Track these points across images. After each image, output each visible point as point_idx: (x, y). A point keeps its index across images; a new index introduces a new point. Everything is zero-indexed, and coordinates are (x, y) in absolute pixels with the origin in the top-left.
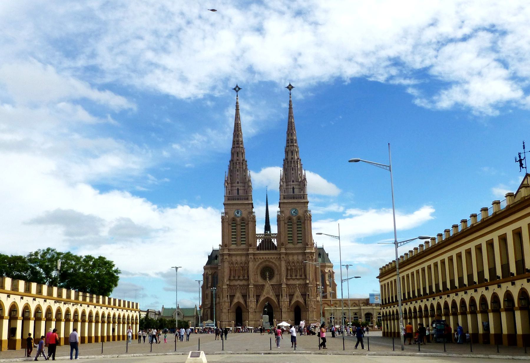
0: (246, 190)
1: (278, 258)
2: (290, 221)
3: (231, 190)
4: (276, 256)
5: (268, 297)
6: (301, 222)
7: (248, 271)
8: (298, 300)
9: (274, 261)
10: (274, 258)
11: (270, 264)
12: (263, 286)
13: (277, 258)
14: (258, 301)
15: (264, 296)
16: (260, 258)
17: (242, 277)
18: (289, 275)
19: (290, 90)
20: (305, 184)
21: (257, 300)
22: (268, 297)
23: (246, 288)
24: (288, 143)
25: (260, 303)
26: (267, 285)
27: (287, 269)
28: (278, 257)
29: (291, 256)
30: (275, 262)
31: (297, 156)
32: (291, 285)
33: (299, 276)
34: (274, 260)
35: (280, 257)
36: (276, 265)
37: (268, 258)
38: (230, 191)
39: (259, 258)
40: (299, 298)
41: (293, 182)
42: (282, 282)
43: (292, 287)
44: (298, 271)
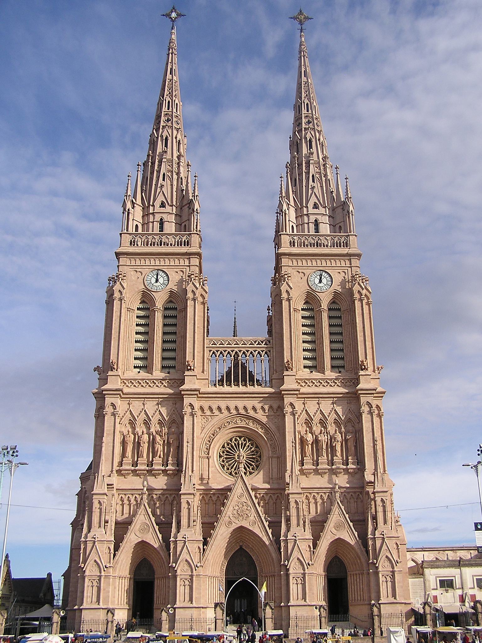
0: (183, 224)
1: (275, 406)
5: (241, 527)
6: (339, 310)
11: (251, 425)
12: (225, 493)
16: (219, 409)
18: (308, 460)
20: (348, 212)
21: (205, 539)
22: (241, 529)
23: (170, 499)
24: (300, 124)
26: (238, 490)
27: (303, 442)
29: (315, 402)
31: (323, 152)
32: (316, 491)
33: (339, 463)
35: (279, 407)
39: (214, 407)
41: (316, 206)
42: (287, 480)
44: (338, 448)
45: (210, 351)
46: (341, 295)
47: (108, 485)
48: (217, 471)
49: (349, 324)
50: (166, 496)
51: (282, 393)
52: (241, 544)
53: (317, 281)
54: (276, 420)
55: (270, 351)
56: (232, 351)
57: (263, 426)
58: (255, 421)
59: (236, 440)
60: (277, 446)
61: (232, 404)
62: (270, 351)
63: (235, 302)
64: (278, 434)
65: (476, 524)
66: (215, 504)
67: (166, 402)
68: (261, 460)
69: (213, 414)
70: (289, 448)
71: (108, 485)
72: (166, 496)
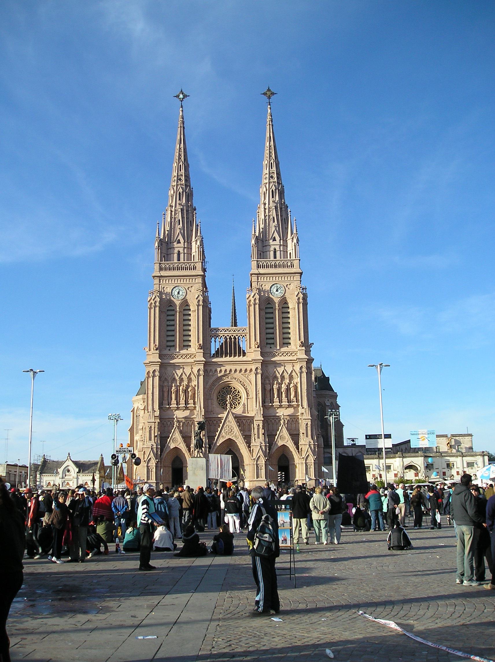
2: (269, 306)
3: (167, 255)
4: (244, 367)
7: (194, 393)
8: (285, 444)
14: (212, 446)
15: (223, 436)
17: (183, 404)
19: (269, 98)
22: (230, 439)
25: (215, 450)
32: (272, 417)
38: (165, 255)
39: (214, 370)
40: (286, 440)
43: (273, 421)
45: (211, 336)
47: (155, 416)
50: (188, 422)
52: (230, 448)
53: (275, 290)
55: (246, 335)
56: (224, 336)
59: (226, 389)
62: (246, 335)
63: (233, 275)
65: (366, 436)
66: (216, 425)
71: (155, 416)
72: (188, 422)
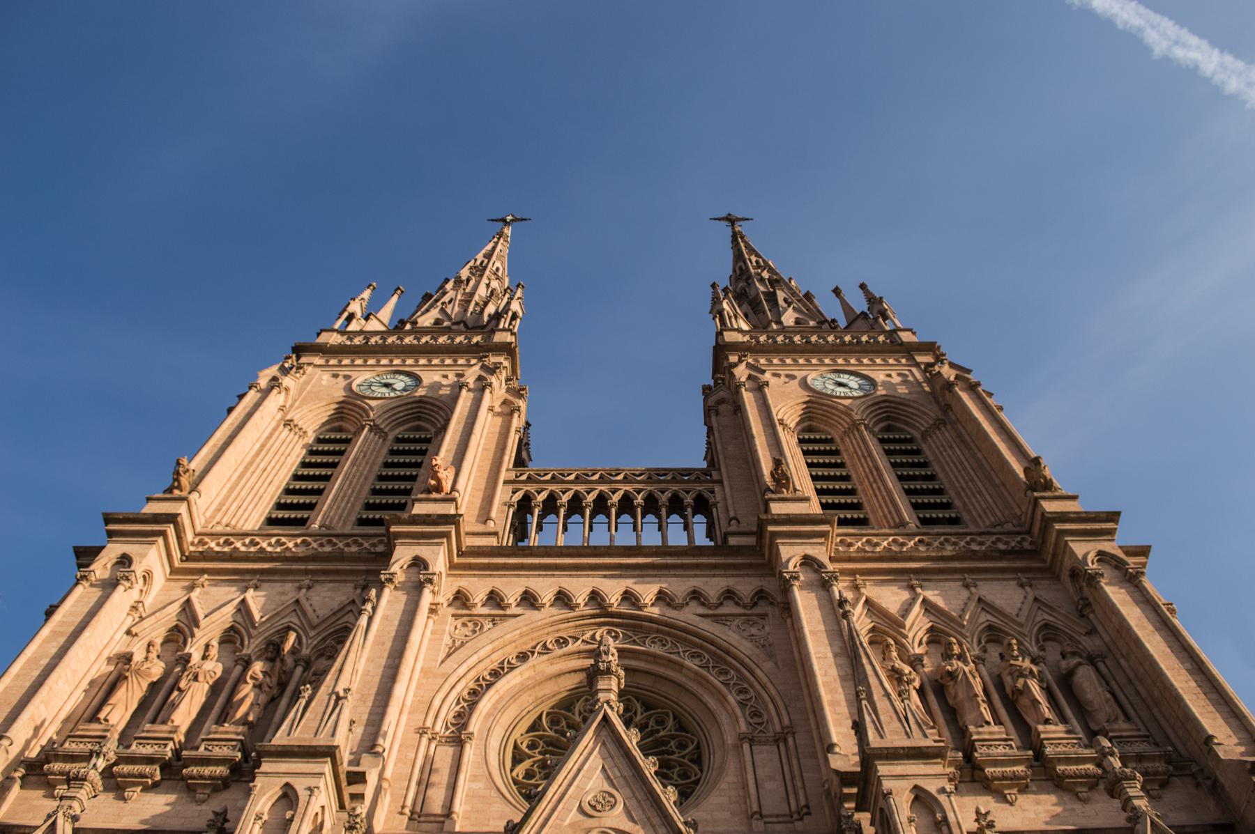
9: (689, 616)
10: (696, 595)
13: (729, 595)
28: (746, 587)
30: (708, 628)
34: (694, 607)
35: (761, 595)
36: (720, 657)
37: (628, 596)
46: (906, 405)
48: (494, 793)
49: (951, 447)
51: (770, 528)
54: (754, 631)
55: (713, 492)
57: (701, 647)
58: (669, 634)
60: (771, 706)
61: (580, 587)
64: (768, 665)
67: (331, 585)
68: (701, 771)
69: (501, 612)
70: (826, 679)
